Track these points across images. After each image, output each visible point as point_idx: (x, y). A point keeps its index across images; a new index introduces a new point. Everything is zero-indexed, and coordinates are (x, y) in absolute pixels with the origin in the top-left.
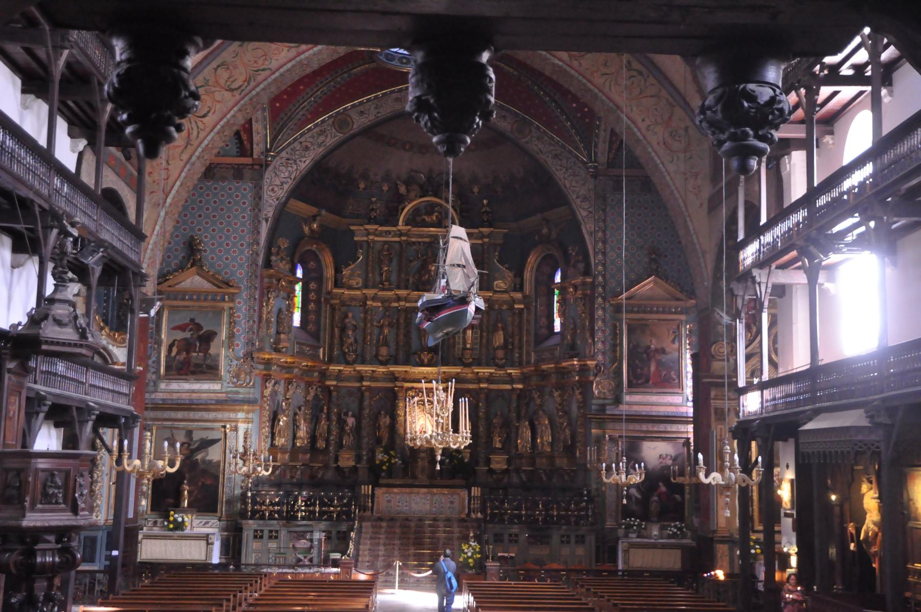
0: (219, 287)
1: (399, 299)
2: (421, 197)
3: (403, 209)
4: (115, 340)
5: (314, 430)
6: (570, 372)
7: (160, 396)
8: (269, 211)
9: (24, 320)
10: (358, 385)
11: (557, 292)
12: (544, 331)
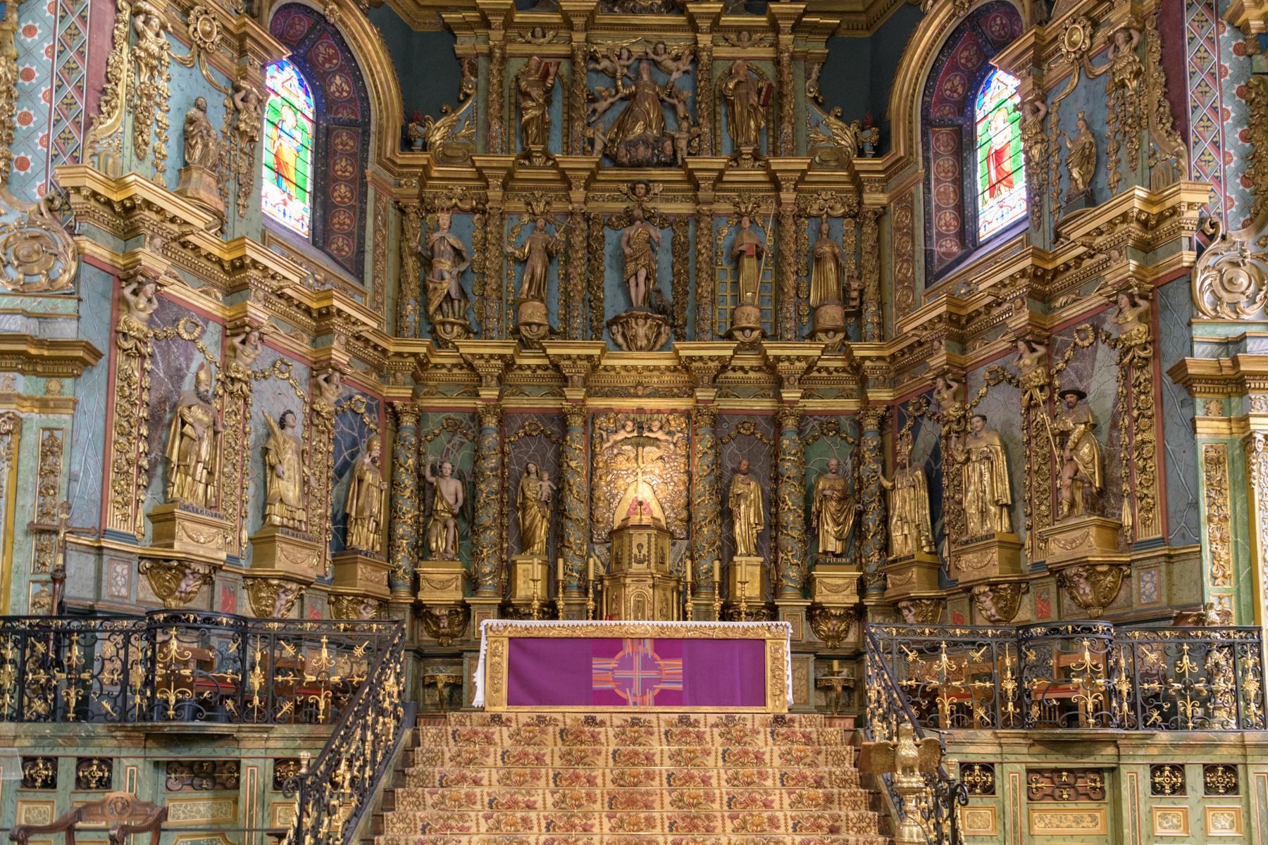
10: (468, 403)
12: (951, 246)
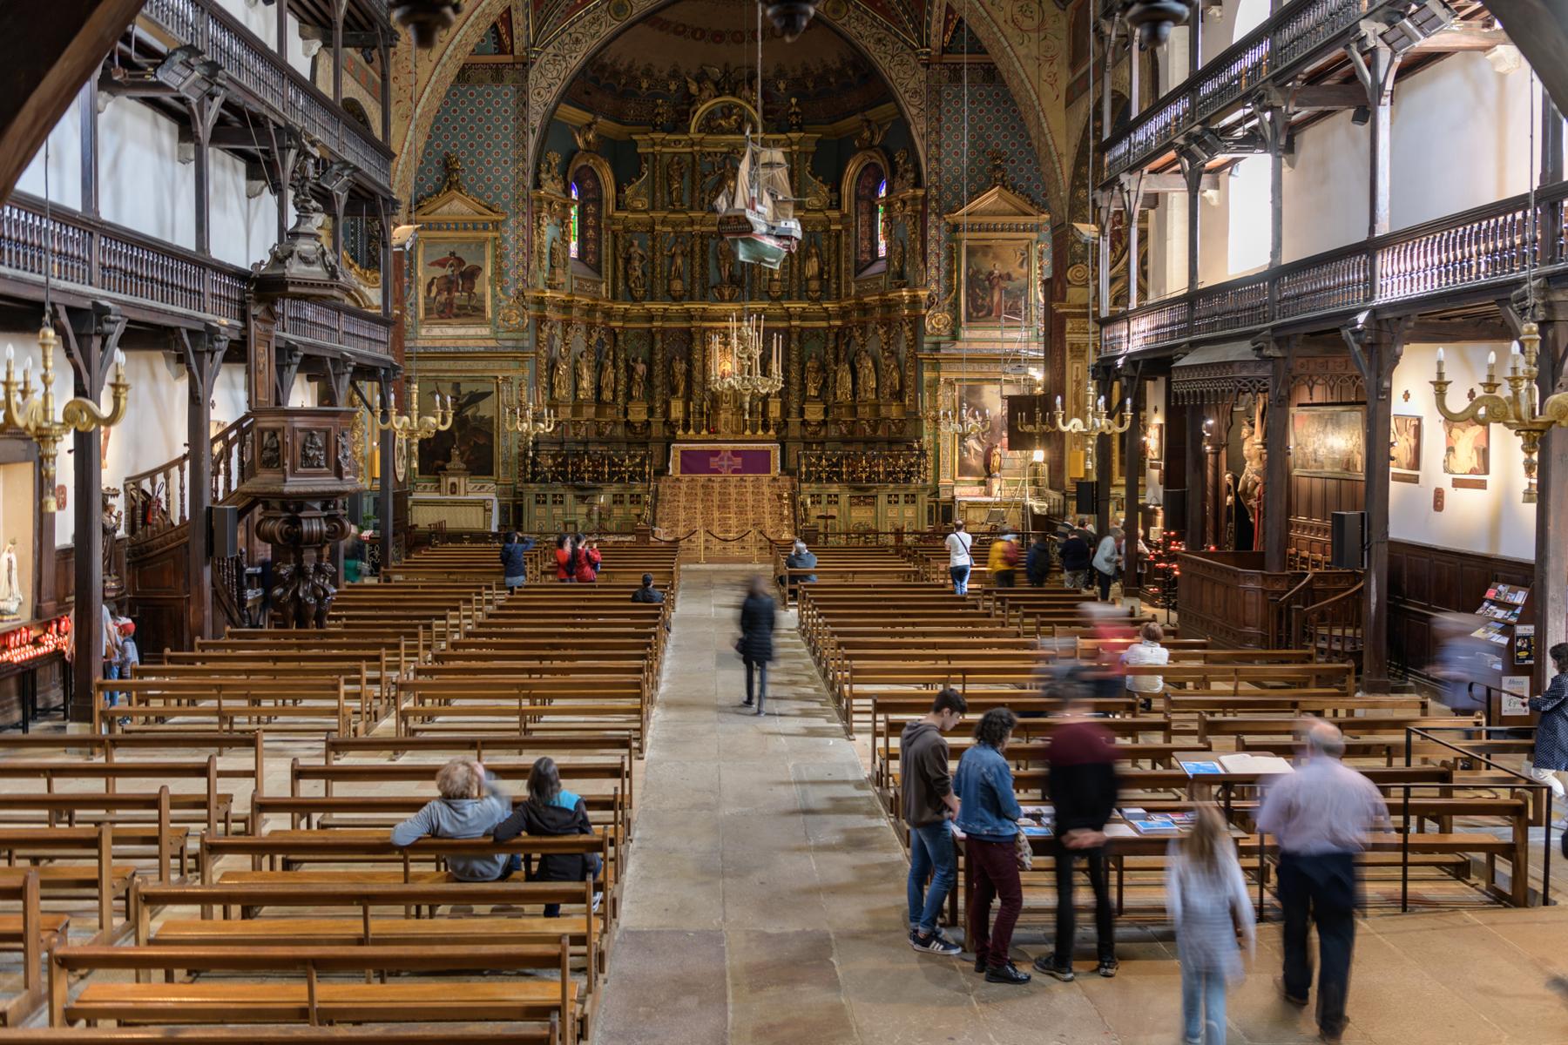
0: (481, 214)
1: (692, 222)
2: (716, 97)
3: (695, 113)
4: (367, 279)
5: (599, 380)
6: (898, 305)
7: (421, 343)
8: (536, 120)
9: (267, 258)
10: (647, 325)
11: (881, 208)
12: (867, 257)
